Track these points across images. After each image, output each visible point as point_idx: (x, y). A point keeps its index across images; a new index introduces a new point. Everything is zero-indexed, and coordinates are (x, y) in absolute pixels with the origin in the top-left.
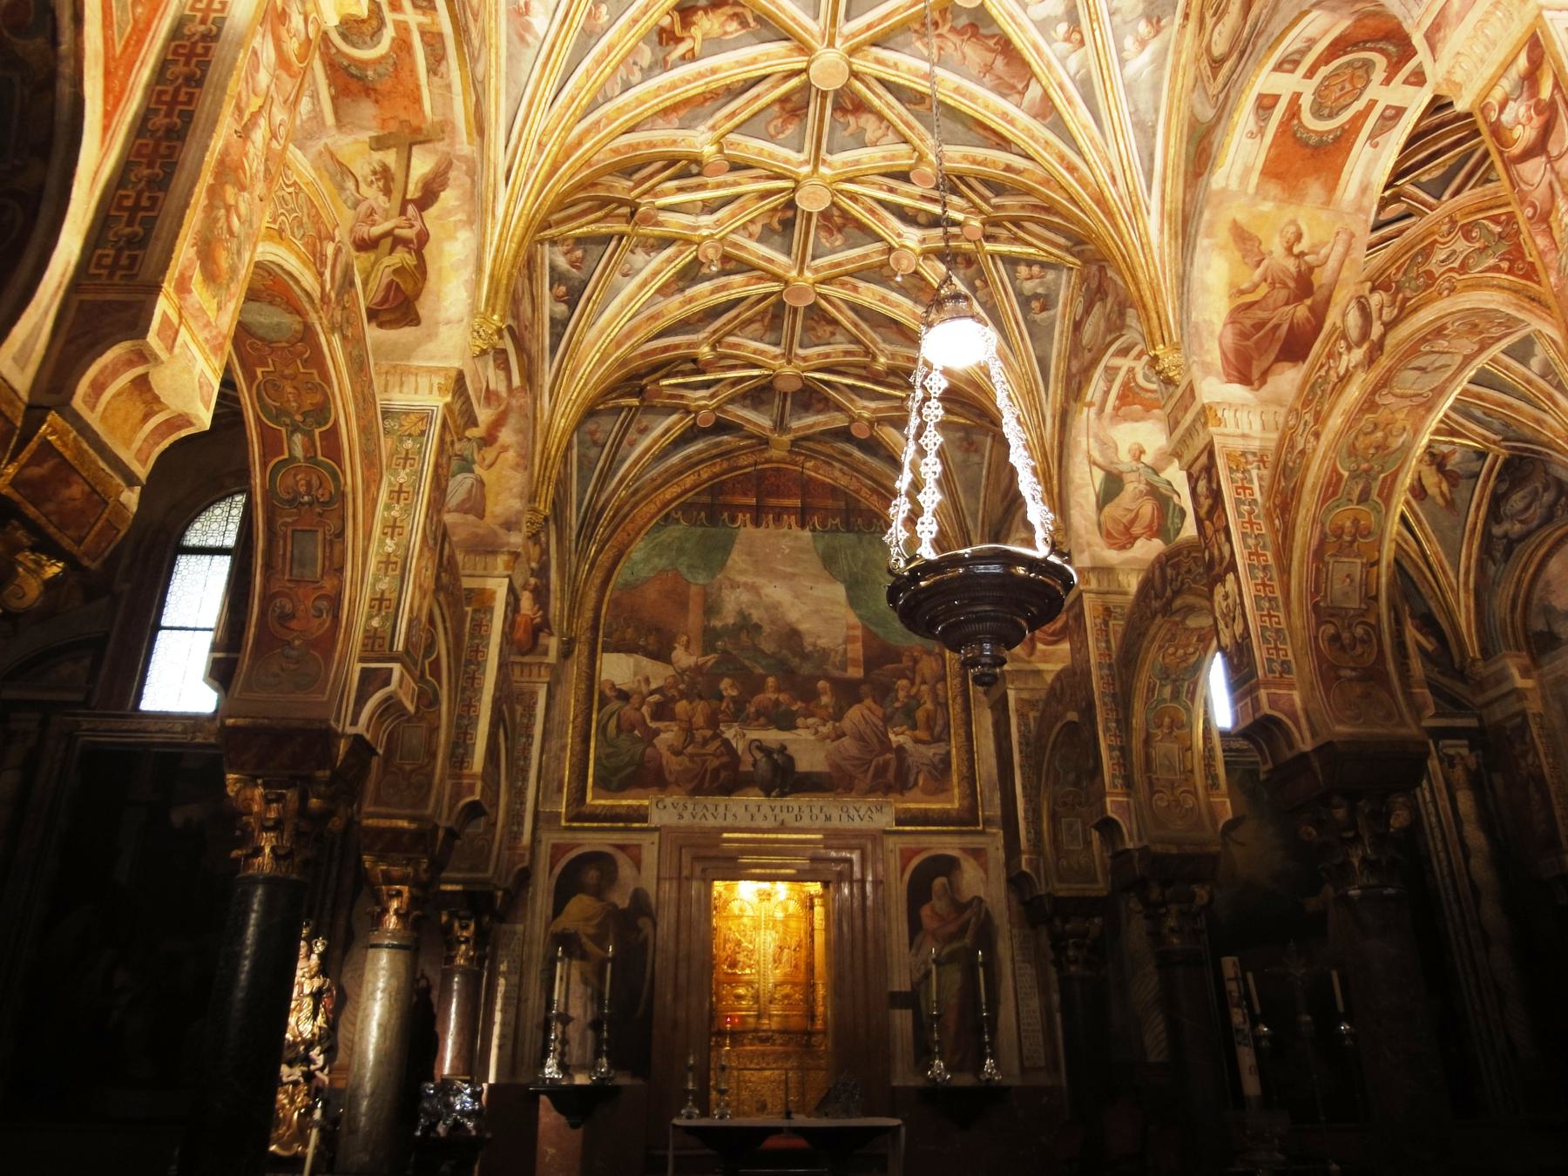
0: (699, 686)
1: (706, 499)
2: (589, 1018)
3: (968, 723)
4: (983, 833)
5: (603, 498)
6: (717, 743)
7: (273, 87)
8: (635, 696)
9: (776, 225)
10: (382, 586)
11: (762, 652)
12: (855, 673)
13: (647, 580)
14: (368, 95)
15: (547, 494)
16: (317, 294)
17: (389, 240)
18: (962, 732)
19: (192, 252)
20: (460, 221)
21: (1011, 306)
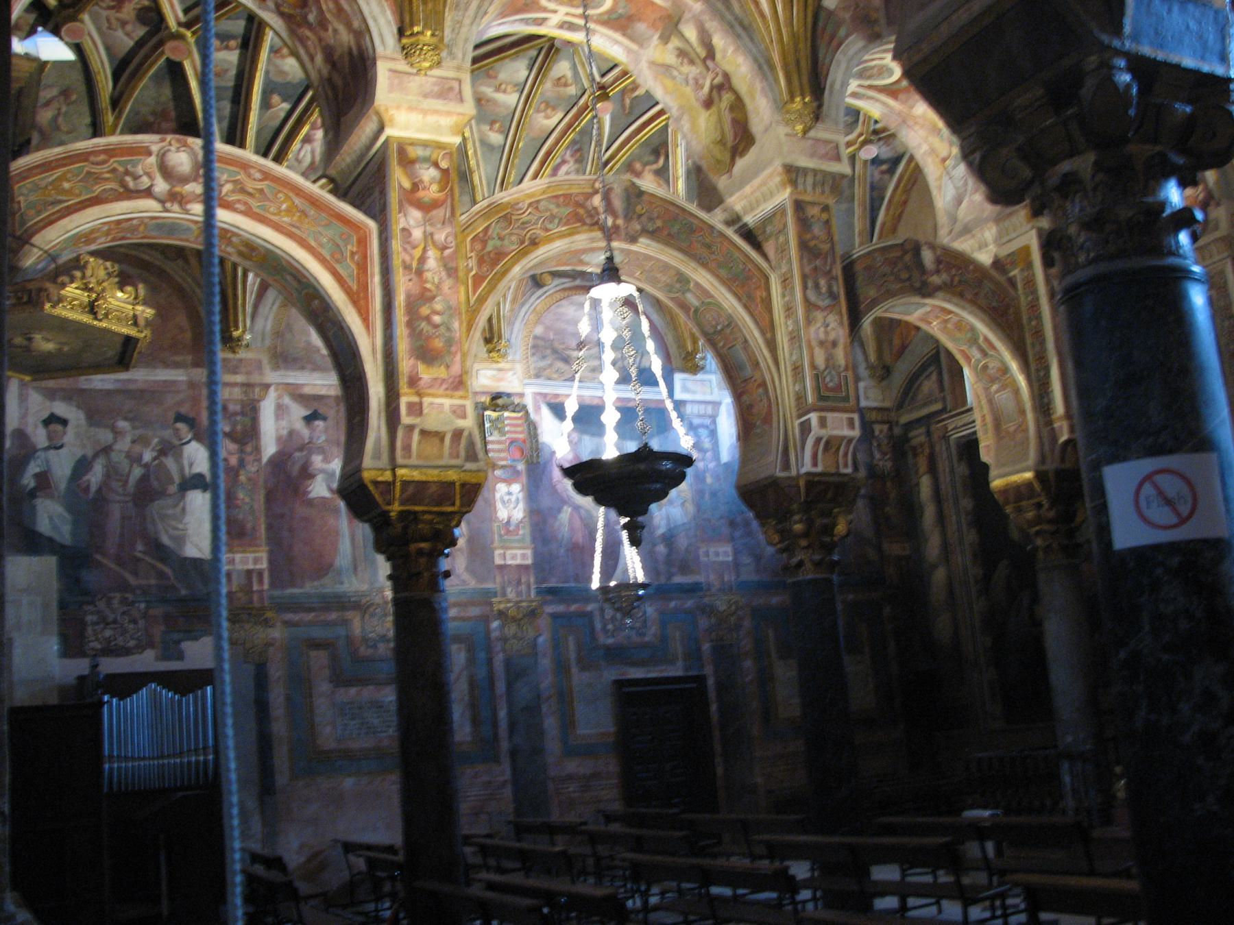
17: (715, 92)
19: (412, 361)
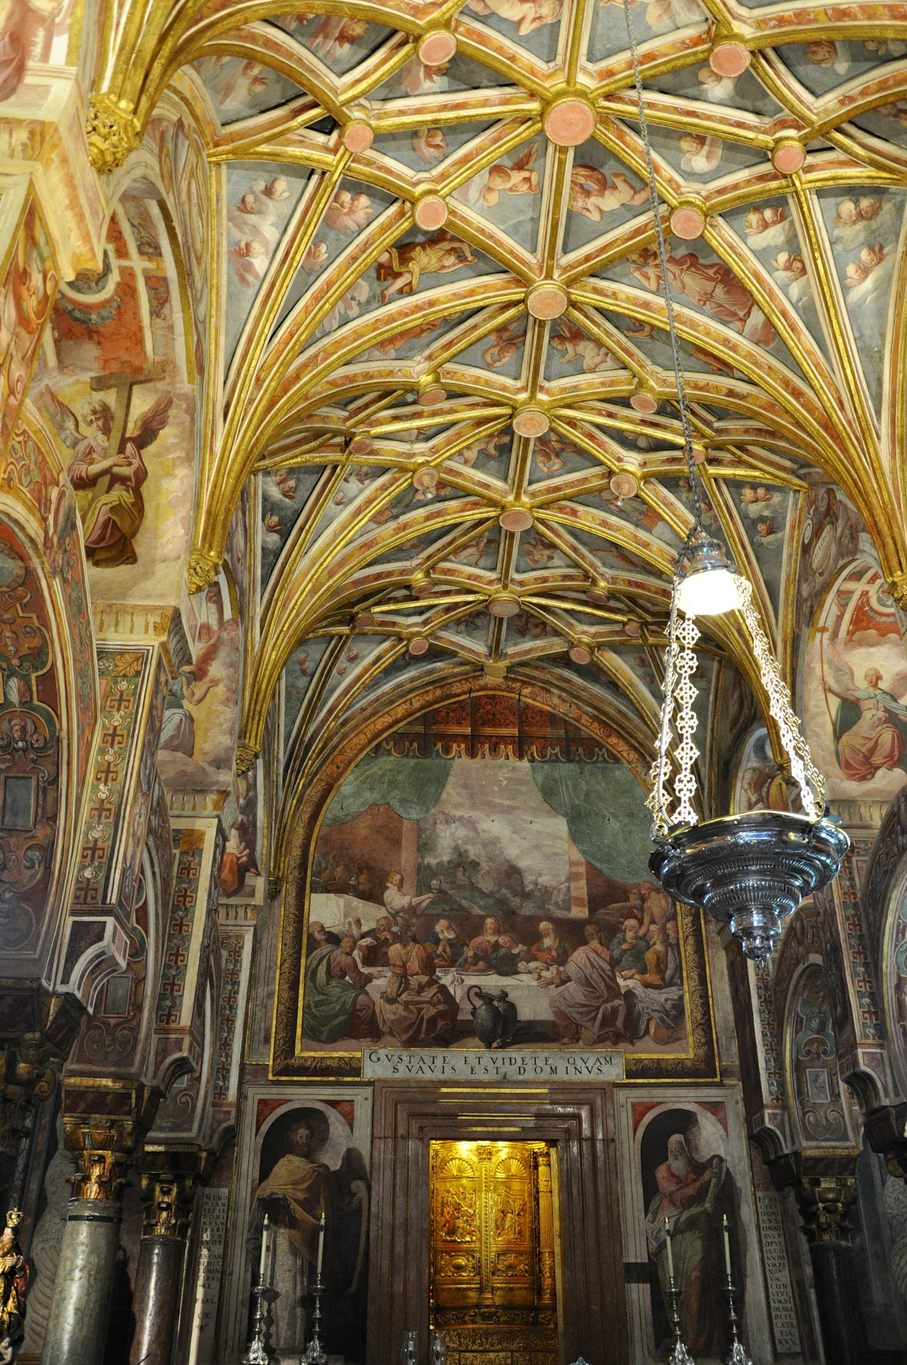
0: (413, 929)
1: (419, 729)
2: (299, 1294)
3: (701, 966)
4: (720, 1085)
5: (311, 730)
6: (434, 989)
7: (13, 344)
8: (346, 940)
9: (492, 451)
10: (96, 834)
11: (480, 891)
12: (579, 912)
13: (359, 815)
14: (90, 338)
15: (258, 729)
16: (40, 540)
17: (107, 478)
18: (694, 975)
20: (179, 458)
21: (737, 530)
